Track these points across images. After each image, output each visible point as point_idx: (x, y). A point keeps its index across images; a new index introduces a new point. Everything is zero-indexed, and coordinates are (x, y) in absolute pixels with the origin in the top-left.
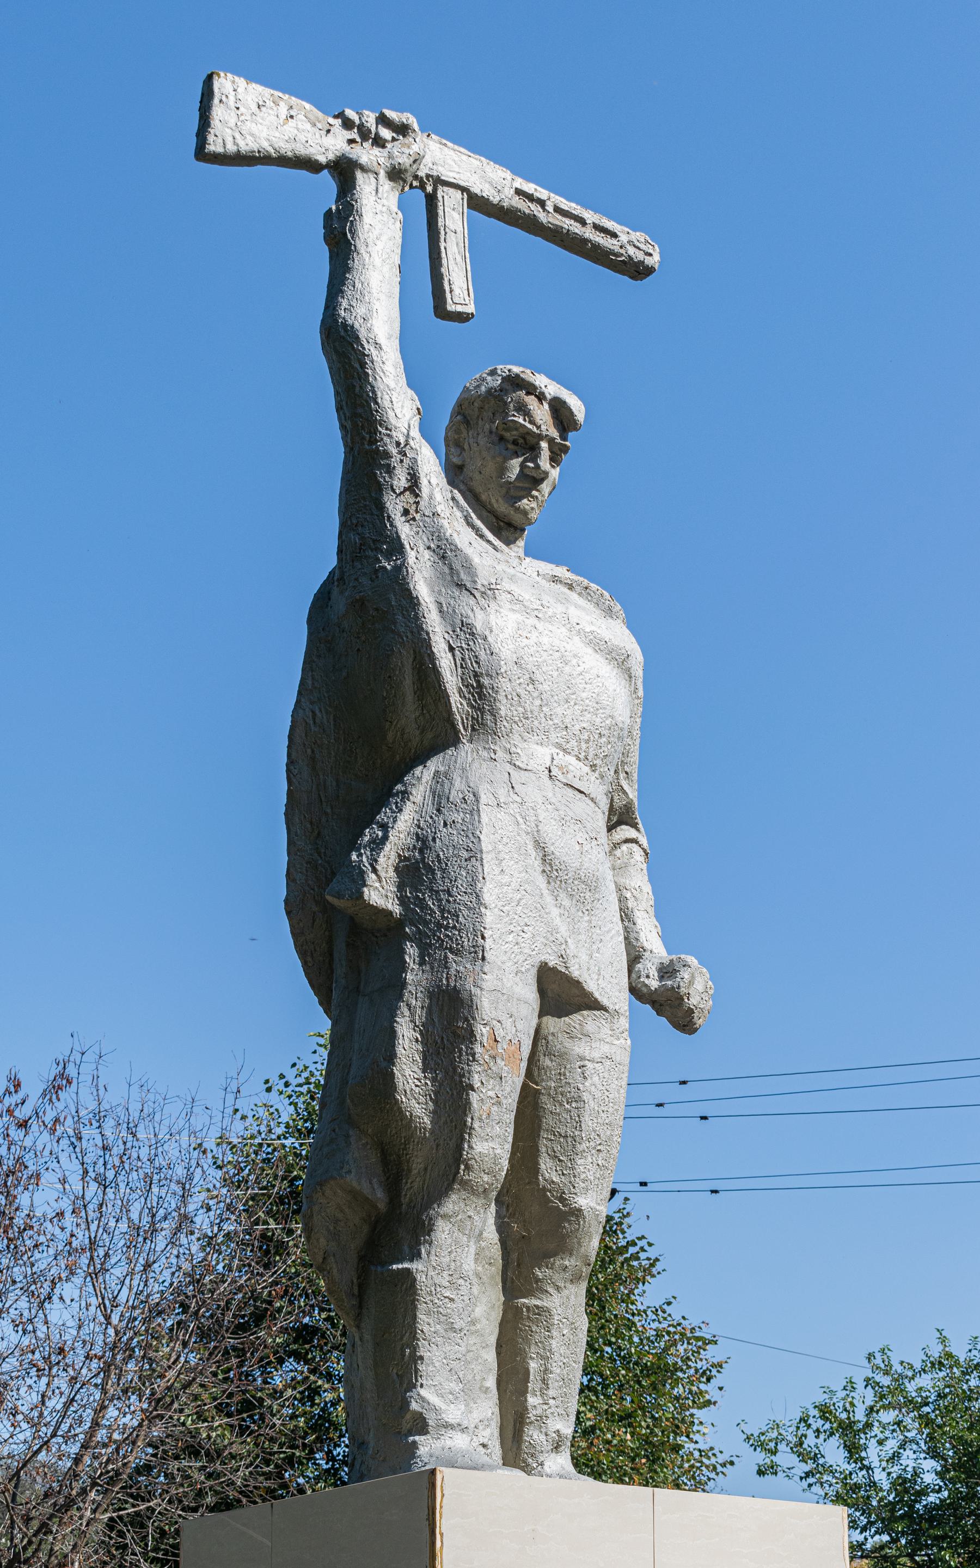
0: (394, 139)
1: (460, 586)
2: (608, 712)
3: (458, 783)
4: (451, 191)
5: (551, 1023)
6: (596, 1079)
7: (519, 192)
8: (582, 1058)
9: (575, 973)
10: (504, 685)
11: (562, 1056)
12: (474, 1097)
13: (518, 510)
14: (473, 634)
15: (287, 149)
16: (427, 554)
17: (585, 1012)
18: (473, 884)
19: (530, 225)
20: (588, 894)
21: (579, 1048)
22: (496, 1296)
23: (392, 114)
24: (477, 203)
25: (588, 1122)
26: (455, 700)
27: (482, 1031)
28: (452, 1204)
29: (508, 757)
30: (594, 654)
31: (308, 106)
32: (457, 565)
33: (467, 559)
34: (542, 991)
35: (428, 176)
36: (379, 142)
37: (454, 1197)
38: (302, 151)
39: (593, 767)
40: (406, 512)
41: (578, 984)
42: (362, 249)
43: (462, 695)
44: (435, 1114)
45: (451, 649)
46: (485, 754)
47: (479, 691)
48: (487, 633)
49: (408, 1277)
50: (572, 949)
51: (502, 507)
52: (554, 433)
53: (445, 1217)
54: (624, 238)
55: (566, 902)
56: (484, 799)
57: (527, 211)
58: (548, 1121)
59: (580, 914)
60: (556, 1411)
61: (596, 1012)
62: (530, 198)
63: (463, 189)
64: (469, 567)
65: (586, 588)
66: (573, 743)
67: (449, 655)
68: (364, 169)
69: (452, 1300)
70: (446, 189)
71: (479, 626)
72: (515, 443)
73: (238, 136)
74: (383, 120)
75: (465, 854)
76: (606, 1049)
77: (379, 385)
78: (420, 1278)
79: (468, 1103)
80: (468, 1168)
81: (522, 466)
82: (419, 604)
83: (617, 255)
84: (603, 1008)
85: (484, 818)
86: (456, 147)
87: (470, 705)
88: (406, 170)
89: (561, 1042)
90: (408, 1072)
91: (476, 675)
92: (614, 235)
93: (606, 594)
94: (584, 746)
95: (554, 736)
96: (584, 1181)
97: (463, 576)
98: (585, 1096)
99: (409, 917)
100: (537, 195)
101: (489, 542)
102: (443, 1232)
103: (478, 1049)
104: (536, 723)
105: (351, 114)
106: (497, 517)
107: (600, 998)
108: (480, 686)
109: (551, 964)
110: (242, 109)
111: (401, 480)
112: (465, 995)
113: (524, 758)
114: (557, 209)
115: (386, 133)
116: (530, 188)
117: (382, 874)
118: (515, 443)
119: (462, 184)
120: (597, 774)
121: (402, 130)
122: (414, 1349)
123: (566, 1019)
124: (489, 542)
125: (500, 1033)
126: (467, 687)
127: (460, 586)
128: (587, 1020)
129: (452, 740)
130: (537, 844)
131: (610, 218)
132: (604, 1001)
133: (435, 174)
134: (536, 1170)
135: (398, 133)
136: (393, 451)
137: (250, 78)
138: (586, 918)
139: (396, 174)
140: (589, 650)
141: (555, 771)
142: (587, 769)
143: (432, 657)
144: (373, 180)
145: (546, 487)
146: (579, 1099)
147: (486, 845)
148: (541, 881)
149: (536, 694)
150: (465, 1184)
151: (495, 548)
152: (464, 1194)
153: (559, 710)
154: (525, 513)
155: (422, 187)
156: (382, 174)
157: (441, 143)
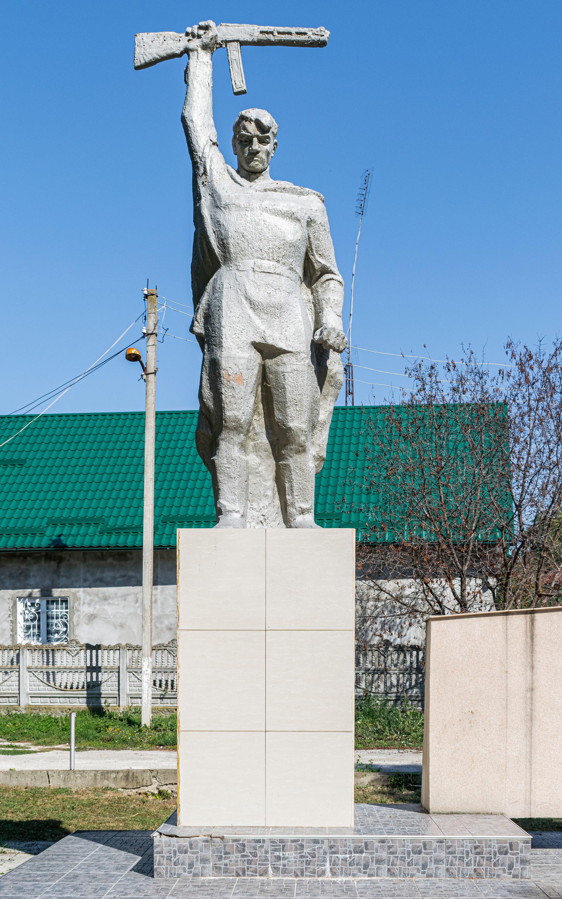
0: (205, 33)
1: (217, 207)
2: (281, 239)
3: (219, 282)
4: (232, 43)
5: (269, 362)
6: (290, 379)
7: (262, 32)
8: (283, 372)
9: (270, 342)
10: (231, 241)
11: (276, 373)
12: (223, 396)
13: (250, 167)
14: (220, 225)
15: (163, 54)
16: (209, 197)
18: (219, 319)
19: (269, 43)
20: (277, 311)
21: (281, 369)
22: (272, 462)
23: (202, 23)
24: (242, 43)
25: (289, 395)
26: (217, 251)
27: (223, 372)
28: (224, 435)
29: (236, 268)
30: (276, 217)
31: (171, 33)
32: (216, 200)
33: (219, 196)
35: (222, 41)
36: (199, 37)
37: (224, 432)
38: (169, 52)
39: (278, 261)
40: (203, 183)
41: (272, 346)
42: (190, 83)
43: (219, 249)
44: (214, 404)
45: (214, 232)
46: (228, 268)
47: (224, 246)
48: (224, 223)
49: (213, 462)
50: (268, 333)
51: (246, 167)
52: (258, 133)
53: (223, 440)
54: (310, 33)
55: (265, 317)
56: (225, 285)
57: (265, 39)
58: (275, 397)
59: (274, 319)
60: (304, 499)
61: (288, 354)
62: (267, 33)
63: (237, 41)
64: (220, 199)
66: (265, 255)
67: (214, 234)
68: (192, 50)
69: (229, 468)
70: (230, 44)
71: (222, 221)
72: (246, 141)
73: (145, 56)
74: (200, 28)
75: (218, 308)
76: (295, 367)
77: (193, 136)
78: (216, 462)
79: (222, 399)
80: (225, 422)
81: (249, 149)
82: (203, 218)
83: (308, 41)
84: (285, 352)
85: (224, 293)
86: (233, 25)
87: (222, 251)
88: (209, 44)
89: (274, 368)
90: (206, 390)
91: (222, 240)
92: (305, 34)
93: (297, 187)
94: (271, 255)
95: (255, 254)
97: (218, 203)
98: (286, 386)
99: (207, 335)
100: (268, 30)
101: (239, 184)
102: (223, 445)
103: (222, 379)
104: (247, 251)
105: (189, 30)
106: (248, 171)
107: (285, 348)
108: (224, 243)
109: (257, 342)
110: (146, 45)
111: (201, 171)
112: (217, 361)
114: (279, 33)
115: (201, 32)
117: (199, 321)
118: (246, 141)
119: (235, 39)
120: (281, 264)
121: (207, 28)
122: (218, 486)
124: (239, 184)
125: (230, 372)
126: (220, 245)
127: (217, 207)
128: (284, 358)
129: (216, 266)
130: (246, 298)
131: (303, 26)
132: (290, 349)
133: (224, 39)
134: (274, 415)
135: (206, 30)
136: (199, 160)
137: (148, 31)
138: (277, 320)
139: (205, 47)
140: (274, 216)
141: (256, 268)
142: (275, 263)
143: (208, 237)
144: (196, 53)
145: (262, 155)
146: (284, 388)
147: (224, 304)
148: (250, 312)
150: (226, 427)
151: (241, 185)
152: (227, 431)
153: (257, 244)
154: (254, 167)
155: (221, 46)
156: (199, 49)
157: (226, 26)
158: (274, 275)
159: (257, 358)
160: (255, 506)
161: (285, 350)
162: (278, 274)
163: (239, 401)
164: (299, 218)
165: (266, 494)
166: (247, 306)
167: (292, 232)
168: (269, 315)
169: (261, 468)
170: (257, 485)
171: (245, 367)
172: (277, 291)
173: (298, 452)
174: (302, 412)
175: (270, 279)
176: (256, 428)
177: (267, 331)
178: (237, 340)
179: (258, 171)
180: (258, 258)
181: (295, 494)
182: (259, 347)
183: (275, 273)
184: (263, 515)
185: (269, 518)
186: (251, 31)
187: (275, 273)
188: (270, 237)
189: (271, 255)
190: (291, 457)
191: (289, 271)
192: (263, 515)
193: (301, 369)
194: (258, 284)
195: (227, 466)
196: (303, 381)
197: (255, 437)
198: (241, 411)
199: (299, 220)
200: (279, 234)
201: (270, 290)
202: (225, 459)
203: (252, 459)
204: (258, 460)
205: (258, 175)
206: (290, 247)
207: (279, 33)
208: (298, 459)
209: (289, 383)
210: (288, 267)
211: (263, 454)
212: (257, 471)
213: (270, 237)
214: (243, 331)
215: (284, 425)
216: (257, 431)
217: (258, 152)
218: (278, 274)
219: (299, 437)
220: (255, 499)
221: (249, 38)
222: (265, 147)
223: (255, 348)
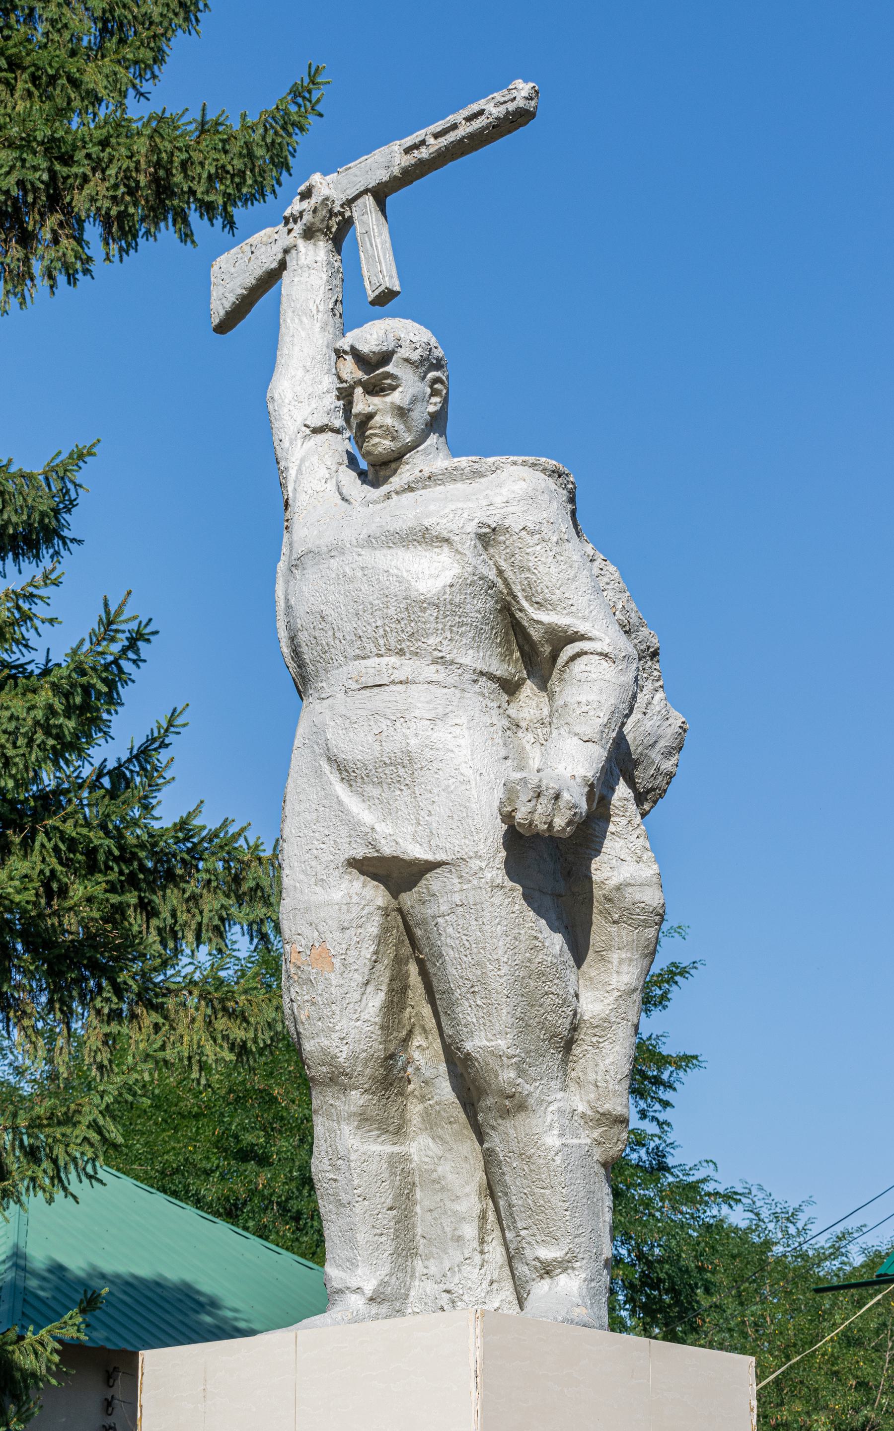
2: (400, 597)
5: (408, 899)
7: (408, 151)
8: (435, 917)
11: (424, 923)
17: (428, 876)
20: (401, 772)
21: (430, 910)
22: (469, 1147)
25: (451, 970)
34: (375, 877)
39: (401, 653)
41: (395, 859)
50: (383, 828)
61: (438, 871)
62: (416, 147)
65: (430, 478)
69: (335, 1180)
76: (457, 898)
96: (466, 1026)
107: (429, 857)
113: (327, 690)
114: (436, 136)
116: (409, 141)
120: (408, 656)
123: (416, 889)
128: (433, 881)
132: (440, 857)
138: (407, 792)
146: (441, 955)
149: (328, 626)
152: (319, 1089)
158: (392, 687)
159: (376, 895)
160: (433, 1270)
161: (427, 862)
162: (401, 682)
163: (327, 1012)
164: (445, 534)
165: (457, 1233)
166: (331, 777)
167: (433, 573)
168: (385, 786)
169: (445, 1169)
170: (435, 1214)
171: (334, 925)
172: (398, 724)
173: (506, 1113)
174: (492, 1009)
175: (379, 698)
176: (423, 1070)
177: (378, 827)
178: (313, 863)
179: (392, 458)
180: (357, 657)
181: (520, 1225)
182: (371, 869)
183: (393, 682)
184: (448, 1292)
185: (465, 1298)
186: (386, 160)
187: (393, 682)
188: (377, 602)
189: (381, 642)
190: (493, 1128)
191: (433, 668)
192: (448, 1292)
193: (471, 901)
194: (354, 719)
195: (332, 1176)
196: (481, 930)
197: (426, 1091)
198: (335, 1036)
199: (447, 540)
200: (395, 588)
201: (384, 724)
202: (325, 1161)
203: (419, 1147)
204: (435, 1149)
205: (393, 466)
206: (424, 610)
207: (436, 136)
208: (512, 1131)
209: (448, 940)
210: (429, 659)
211: (446, 1131)
212: (435, 1176)
213: (377, 602)
214: (326, 840)
215: (458, 1049)
216: (428, 1074)
217: (370, 416)
218: (401, 682)
219: (497, 1076)
220: (434, 1250)
221: (383, 176)
222: (388, 399)
223: (362, 873)
